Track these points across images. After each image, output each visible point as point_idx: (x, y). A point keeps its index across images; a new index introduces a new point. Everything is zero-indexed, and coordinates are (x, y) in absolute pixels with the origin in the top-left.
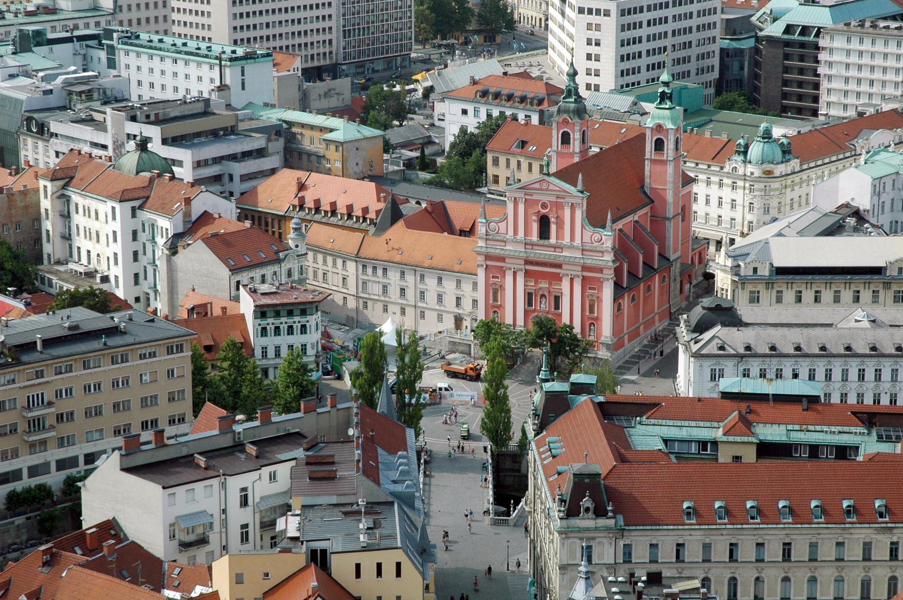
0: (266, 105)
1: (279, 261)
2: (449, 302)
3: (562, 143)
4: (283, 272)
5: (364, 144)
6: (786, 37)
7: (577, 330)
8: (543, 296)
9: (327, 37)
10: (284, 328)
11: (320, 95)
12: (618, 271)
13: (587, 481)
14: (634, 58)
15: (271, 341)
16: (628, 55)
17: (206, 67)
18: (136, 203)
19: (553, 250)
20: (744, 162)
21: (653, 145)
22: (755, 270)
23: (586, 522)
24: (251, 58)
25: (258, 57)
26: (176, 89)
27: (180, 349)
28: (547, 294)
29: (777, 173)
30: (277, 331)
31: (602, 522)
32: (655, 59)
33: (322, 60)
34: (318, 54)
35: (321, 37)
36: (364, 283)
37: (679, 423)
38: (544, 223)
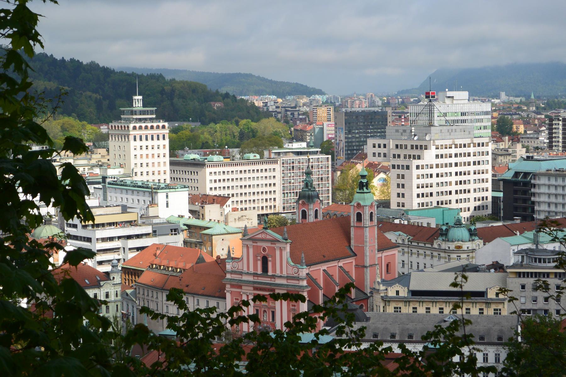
0: (179, 216)
4: (102, 294)
6: (514, 179)
8: (265, 311)
9: (272, 196)
11: (235, 219)
14: (427, 196)
16: (423, 194)
19: (270, 279)
21: (356, 217)
22: (398, 292)
24: (173, 188)
25: (178, 188)
28: (266, 310)
29: (465, 248)
34: (267, 207)
35: (268, 196)
36: (167, 307)
38: (265, 261)
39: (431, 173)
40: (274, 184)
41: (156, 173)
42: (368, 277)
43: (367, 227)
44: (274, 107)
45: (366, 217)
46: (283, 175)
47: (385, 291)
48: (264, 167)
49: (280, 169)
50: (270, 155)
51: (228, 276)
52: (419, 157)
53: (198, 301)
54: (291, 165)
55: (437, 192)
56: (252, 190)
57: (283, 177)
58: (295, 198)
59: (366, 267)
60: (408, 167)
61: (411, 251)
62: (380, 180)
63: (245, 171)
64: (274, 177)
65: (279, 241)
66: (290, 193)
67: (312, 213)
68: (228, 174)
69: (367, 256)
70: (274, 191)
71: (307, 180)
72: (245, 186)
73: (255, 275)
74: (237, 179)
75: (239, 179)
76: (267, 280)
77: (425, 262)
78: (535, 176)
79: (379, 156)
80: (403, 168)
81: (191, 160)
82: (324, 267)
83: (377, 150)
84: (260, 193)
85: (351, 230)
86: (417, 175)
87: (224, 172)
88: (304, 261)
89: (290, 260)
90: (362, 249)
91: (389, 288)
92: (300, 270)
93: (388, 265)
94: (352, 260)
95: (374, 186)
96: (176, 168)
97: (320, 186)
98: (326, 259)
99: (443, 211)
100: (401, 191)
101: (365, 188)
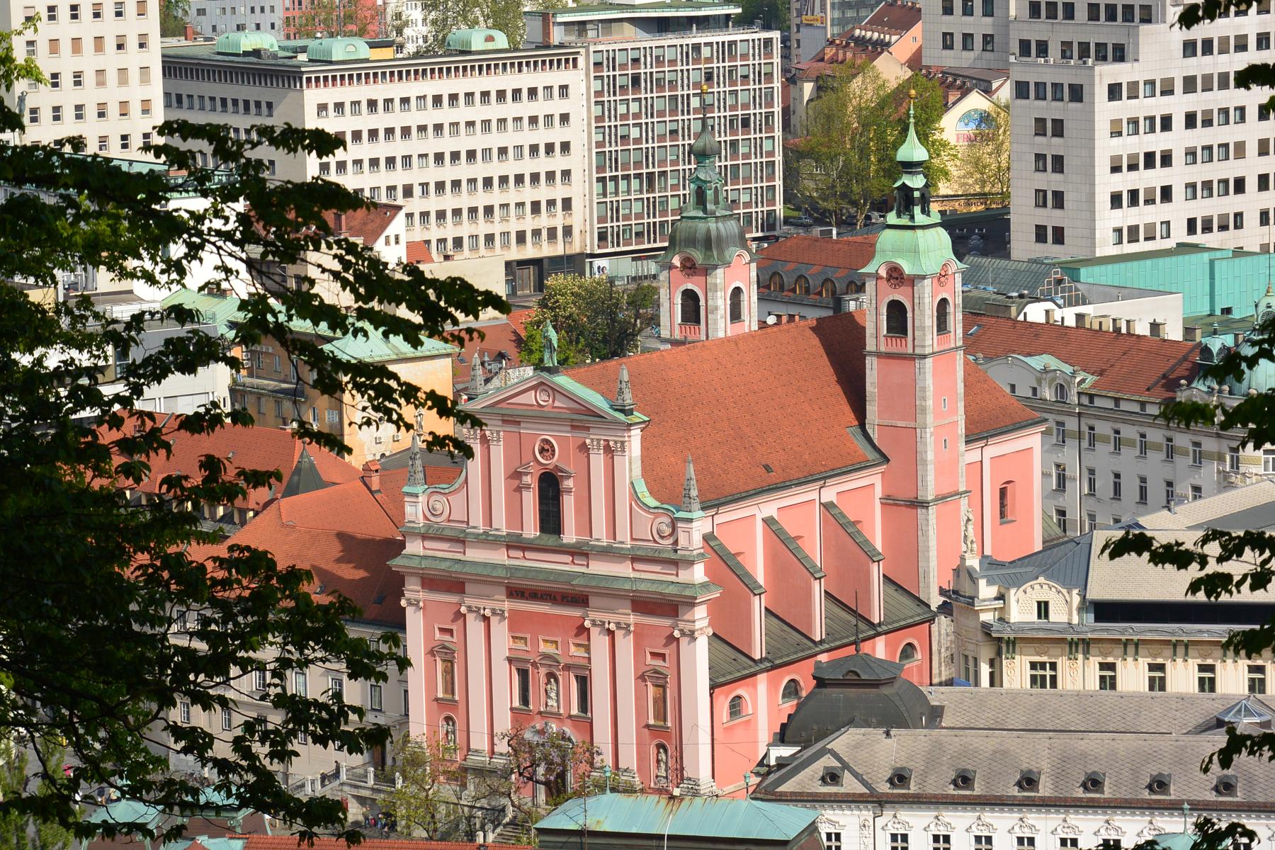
3: (685, 319)
7: (629, 759)
16: (1134, 195)
19: (568, 559)
22: (1043, 608)
33: (545, 244)
35: (543, 193)
39: (1166, 112)
40: (565, 147)
41: (113, 110)
42: (933, 543)
43: (924, 357)
45: (925, 317)
46: (596, 111)
47: (999, 604)
48: (526, 80)
49: (588, 89)
50: (546, 33)
51: (414, 547)
52: (1120, 54)
54: (630, 72)
55: (1187, 186)
56: (480, 170)
57: (599, 119)
58: (645, 196)
59: (924, 505)
60: (1077, 93)
61: (1092, 428)
62: (966, 117)
63: (453, 98)
64: (565, 118)
66: (627, 177)
67: (720, 302)
68: (386, 109)
69: (925, 462)
70: (566, 174)
71: (702, 176)
72: (455, 156)
73: (515, 543)
74: (422, 128)
75: (430, 129)
77: (1143, 473)
79: (965, 48)
80: (1058, 98)
81: (246, 54)
82: (769, 507)
84: (512, 180)
85: (868, 366)
86: (1113, 122)
87: (372, 104)
88: (694, 493)
89: (642, 488)
90: (910, 437)
91: (1013, 595)
92: (679, 525)
93: (1003, 492)
94: (874, 480)
95: (944, 145)
96: (188, 87)
97: (742, 150)
98: (774, 477)
99: (1212, 262)
100: (1050, 181)
101: (917, 210)
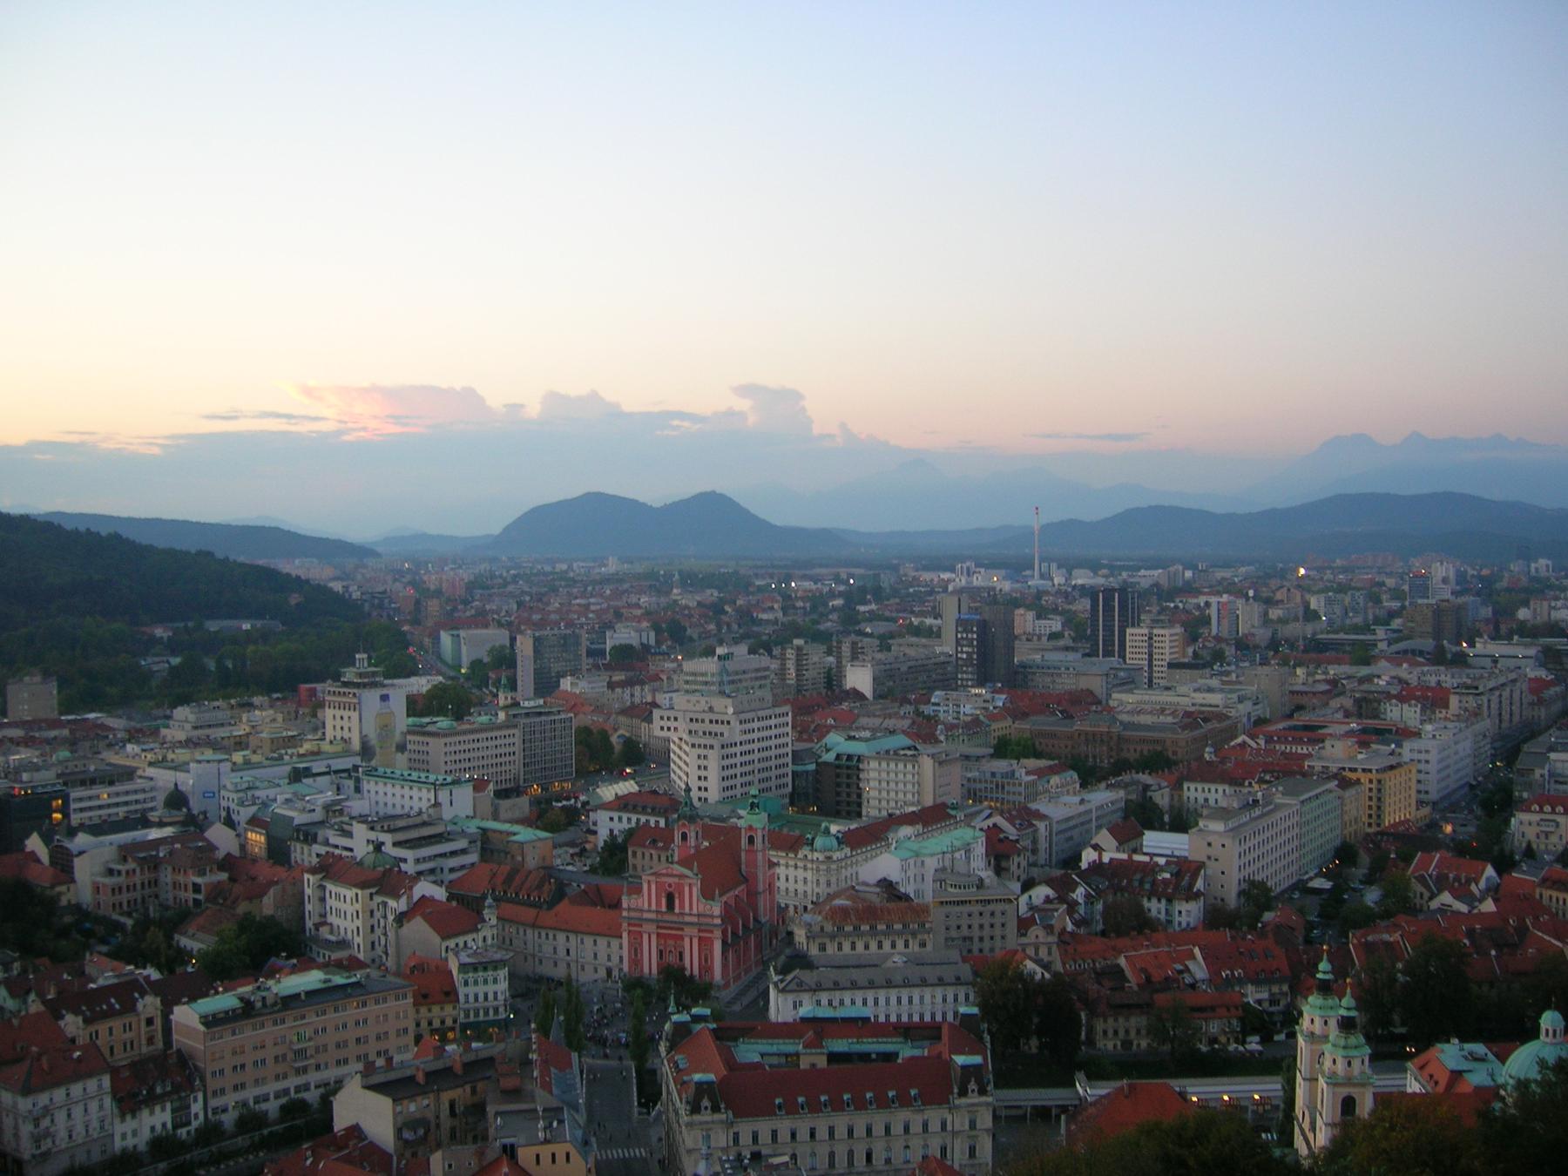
0: (467, 817)
1: (477, 930)
2: (602, 958)
5: (538, 844)
7: (696, 972)
10: (480, 980)
12: (724, 932)
13: (705, 1087)
15: (471, 990)
17: (425, 791)
18: (374, 890)
20: (812, 850)
23: (706, 1117)
26: (403, 807)
27: (405, 996)
29: (835, 858)
30: (476, 983)
31: (717, 1117)
32: (745, 779)
36: (540, 946)
37: (770, 1041)
38: (670, 898)
44: (359, 593)
51: (625, 914)
53: (582, 940)
62: (619, 737)
65: (687, 877)
76: (675, 918)
78: (860, 759)
83: (665, 723)
90: (755, 877)
